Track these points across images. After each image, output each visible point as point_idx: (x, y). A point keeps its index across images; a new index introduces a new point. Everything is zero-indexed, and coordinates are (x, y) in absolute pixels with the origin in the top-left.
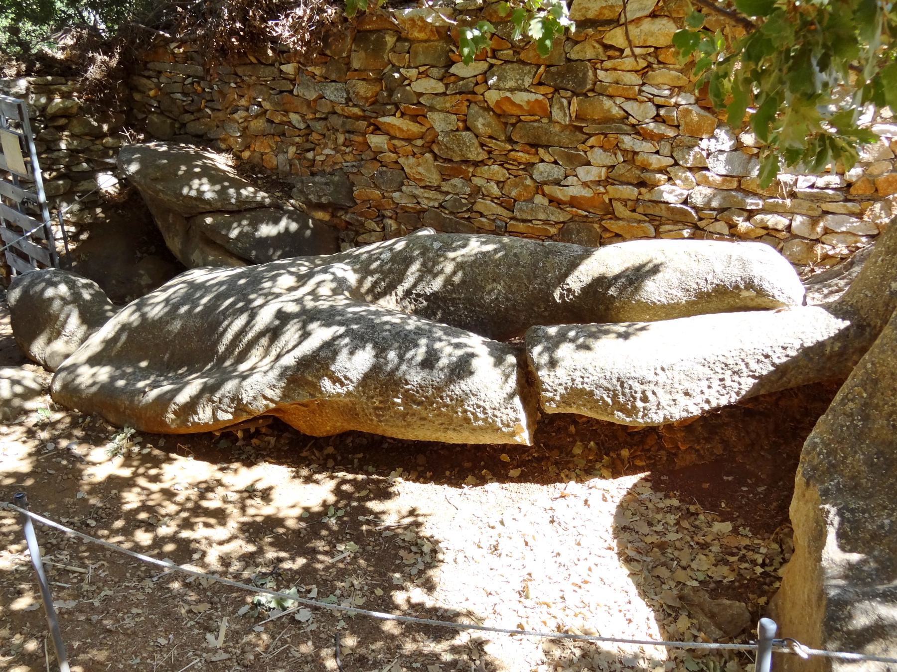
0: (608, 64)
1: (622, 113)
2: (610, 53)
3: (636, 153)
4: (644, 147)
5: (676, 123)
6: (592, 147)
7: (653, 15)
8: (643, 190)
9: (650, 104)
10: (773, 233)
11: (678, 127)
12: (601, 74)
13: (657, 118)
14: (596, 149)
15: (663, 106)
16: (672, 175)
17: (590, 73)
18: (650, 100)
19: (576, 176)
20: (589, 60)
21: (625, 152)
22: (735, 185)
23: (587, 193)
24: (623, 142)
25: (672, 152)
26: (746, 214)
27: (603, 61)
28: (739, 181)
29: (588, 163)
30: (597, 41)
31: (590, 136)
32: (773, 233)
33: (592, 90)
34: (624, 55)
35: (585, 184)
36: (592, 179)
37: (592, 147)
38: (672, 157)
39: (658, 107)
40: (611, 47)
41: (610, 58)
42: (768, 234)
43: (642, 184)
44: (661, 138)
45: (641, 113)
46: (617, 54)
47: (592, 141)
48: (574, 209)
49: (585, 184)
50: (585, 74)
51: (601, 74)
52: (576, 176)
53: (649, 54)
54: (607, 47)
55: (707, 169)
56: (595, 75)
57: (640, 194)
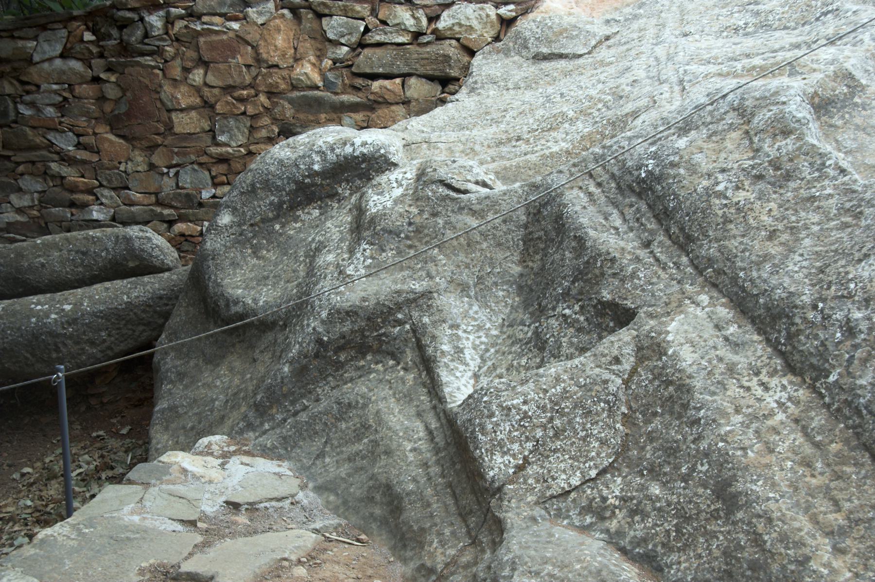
0: (27, 98)
1: (46, 141)
2: (28, 87)
3: (63, 178)
4: (68, 172)
5: (96, 149)
6: (22, 175)
7: (62, 56)
8: (74, 210)
9: (71, 134)
10: (189, 238)
11: (98, 152)
12: (22, 109)
13: (78, 145)
14: (26, 177)
15: (82, 135)
16: (99, 195)
17: (11, 106)
18: (70, 130)
19: (9, 203)
20: (9, 95)
21: (53, 177)
22: (153, 199)
23: (19, 218)
24: (50, 167)
25: (96, 175)
26: (165, 225)
27: (21, 96)
28: (157, 197)
29: (20, 190)
30: (13, 78)
31: (18, 164)
32: (189, 238)
33: (15, 122)
34: (41, 90)
35: (20, 211)
36: (26, 204)
37: (22, 175)
38: (97, 180)
39: (78, 136)
40: (28, 83)
41: (28, 93)
42: (186, 240)
43: (72, 204)
44: (84, 162)
45: (66, 143)
46: (34, 88)
47: (21, 168)
48: (12, 235)
49: (20, 211)
50: (6, 107)
51: (22, 109)
52: (9, 203)
53: (64, 90)
54: (23, 83)
55: (128, 188)
56: (16, 109)
57: (72, 215)
